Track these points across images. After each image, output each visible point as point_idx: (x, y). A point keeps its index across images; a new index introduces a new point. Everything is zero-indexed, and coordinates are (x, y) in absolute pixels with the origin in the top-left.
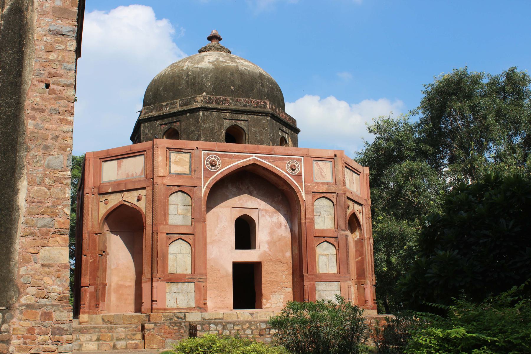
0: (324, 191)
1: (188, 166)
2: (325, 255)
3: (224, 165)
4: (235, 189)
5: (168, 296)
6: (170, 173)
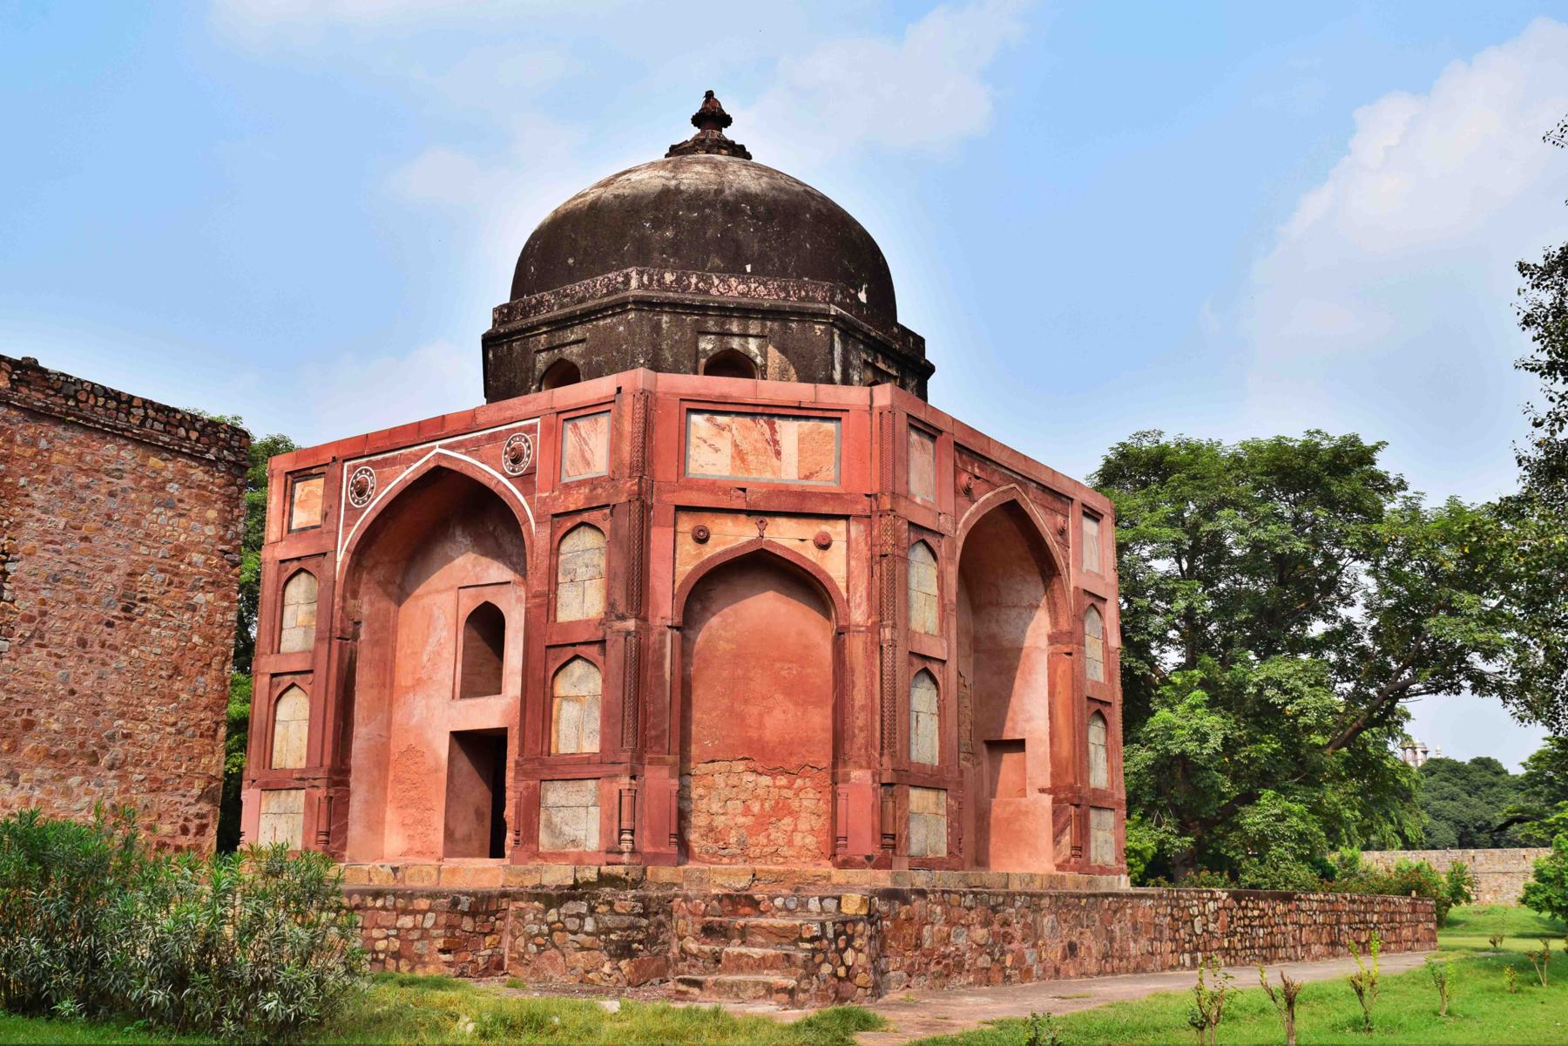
0: (580, 505)
1: (318, 510)
2: (577, 699)
3: (383, 483)
4: (467, 541)
5: (265, 823)
6: (289, 531)
